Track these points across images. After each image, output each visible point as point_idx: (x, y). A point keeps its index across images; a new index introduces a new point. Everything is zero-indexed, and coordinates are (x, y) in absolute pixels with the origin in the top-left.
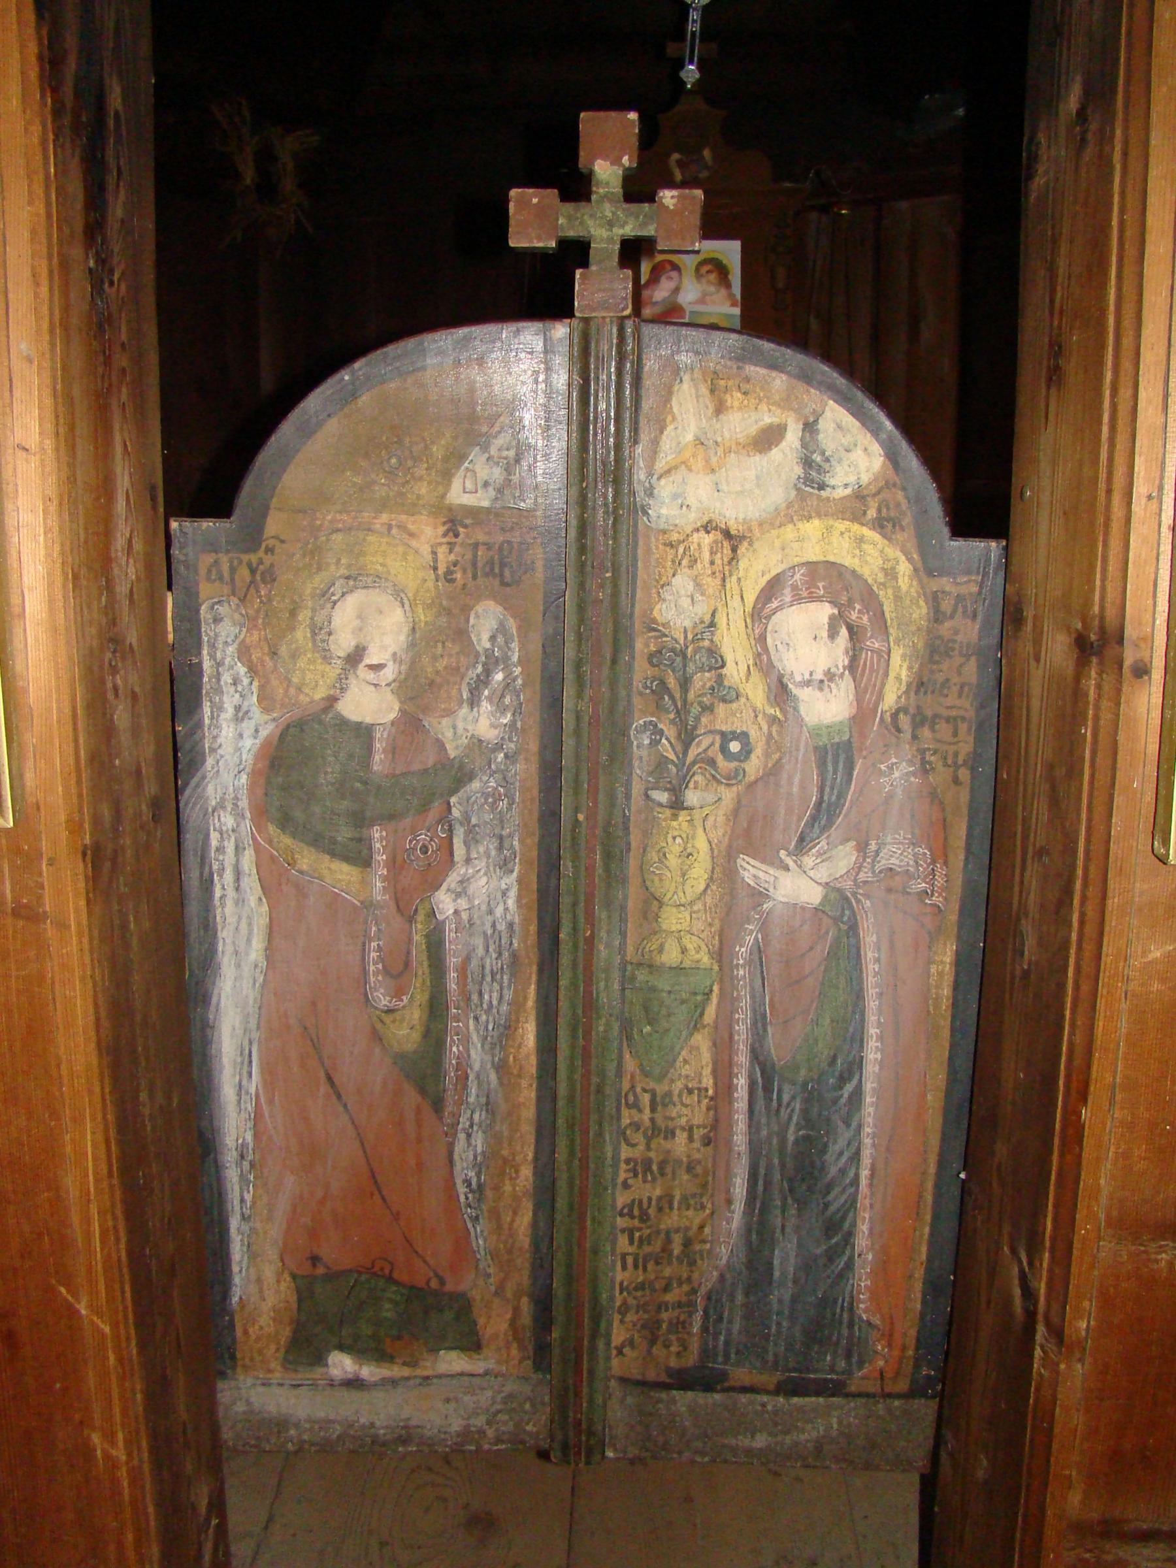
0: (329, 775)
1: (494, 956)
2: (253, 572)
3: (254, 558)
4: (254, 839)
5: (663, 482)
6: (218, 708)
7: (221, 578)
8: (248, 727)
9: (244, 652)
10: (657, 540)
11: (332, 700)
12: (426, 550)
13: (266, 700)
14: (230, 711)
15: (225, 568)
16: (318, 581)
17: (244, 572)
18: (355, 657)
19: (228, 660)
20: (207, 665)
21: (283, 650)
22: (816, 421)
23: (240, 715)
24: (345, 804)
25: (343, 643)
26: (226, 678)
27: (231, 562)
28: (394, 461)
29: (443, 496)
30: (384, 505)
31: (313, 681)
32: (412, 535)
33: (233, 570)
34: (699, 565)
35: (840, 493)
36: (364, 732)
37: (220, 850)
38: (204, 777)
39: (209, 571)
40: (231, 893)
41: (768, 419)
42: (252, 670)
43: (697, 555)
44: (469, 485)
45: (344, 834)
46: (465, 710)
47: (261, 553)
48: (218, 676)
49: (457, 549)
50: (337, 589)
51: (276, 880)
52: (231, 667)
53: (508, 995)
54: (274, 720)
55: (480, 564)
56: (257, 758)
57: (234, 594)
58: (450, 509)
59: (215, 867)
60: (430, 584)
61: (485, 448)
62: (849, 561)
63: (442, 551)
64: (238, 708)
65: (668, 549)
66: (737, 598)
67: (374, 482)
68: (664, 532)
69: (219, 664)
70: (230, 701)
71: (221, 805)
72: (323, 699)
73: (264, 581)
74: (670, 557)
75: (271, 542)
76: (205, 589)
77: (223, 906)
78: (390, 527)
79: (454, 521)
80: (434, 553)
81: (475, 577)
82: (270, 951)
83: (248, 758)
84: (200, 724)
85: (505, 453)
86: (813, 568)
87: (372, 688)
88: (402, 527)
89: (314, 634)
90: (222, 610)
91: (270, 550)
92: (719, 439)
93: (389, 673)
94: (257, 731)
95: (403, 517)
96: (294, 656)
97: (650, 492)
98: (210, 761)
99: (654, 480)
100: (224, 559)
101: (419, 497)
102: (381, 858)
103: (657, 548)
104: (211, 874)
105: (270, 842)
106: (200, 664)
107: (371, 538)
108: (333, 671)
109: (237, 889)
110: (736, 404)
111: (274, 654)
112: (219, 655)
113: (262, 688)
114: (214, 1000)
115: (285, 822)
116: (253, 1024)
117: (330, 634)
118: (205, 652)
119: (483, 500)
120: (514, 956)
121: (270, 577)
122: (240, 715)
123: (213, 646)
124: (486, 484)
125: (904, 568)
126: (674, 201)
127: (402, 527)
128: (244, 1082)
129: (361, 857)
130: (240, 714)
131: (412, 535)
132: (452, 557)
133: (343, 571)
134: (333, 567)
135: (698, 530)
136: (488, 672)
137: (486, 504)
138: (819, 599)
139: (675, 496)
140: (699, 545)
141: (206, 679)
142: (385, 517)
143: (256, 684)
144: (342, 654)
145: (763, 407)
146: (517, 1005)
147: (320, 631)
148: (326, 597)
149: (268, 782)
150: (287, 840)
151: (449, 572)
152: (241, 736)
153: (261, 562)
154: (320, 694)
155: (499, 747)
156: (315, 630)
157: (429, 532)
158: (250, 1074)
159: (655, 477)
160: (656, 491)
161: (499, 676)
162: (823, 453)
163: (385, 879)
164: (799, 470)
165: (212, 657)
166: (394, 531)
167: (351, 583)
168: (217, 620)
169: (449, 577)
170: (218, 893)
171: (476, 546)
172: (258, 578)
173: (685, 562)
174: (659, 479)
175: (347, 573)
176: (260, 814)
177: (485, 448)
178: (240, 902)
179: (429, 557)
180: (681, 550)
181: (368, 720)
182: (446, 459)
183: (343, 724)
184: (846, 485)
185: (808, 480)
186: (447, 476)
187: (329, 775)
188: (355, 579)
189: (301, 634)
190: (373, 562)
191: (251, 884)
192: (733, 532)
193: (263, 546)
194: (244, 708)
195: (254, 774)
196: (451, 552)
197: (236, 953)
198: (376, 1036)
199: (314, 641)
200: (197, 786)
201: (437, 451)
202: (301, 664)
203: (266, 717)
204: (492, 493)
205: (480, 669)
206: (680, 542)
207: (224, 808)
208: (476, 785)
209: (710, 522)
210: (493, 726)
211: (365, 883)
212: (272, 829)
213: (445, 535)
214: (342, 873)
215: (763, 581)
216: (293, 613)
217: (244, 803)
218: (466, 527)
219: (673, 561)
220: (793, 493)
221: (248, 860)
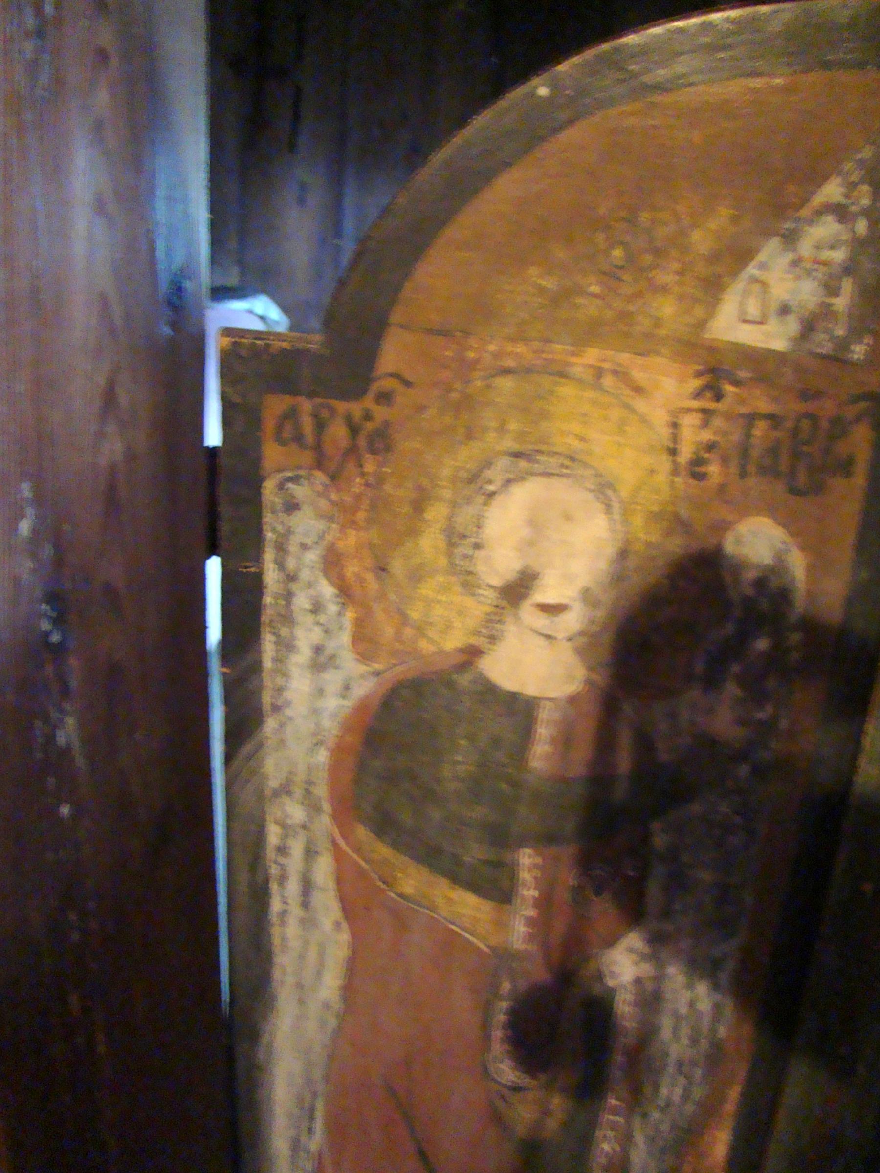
0: (459, 763)
1: (685, 1041)
2: (354, 430)
3: (356, 409)
4: (334, 843)
6: (287, 646)
7: (298, 439)
8: (333, 679)
9: (332, 563)
11: (473, 653)
12: (660, 418)
13: (365, 642)
14: (303, 655)
15: (308, 425)
16: (465, 457)
17: (338, 432)
18: (517, 590)
19: (305, 575)
20: (271, 576)
21: (397, 566)
23: (321, 660)
24: (479, 813)
25: (500, 563)
26: (302, 601)
27: (316, 416)
28: (618, 253)
29: (702, 324)
30: (591, 333)
31: (444, 621)
32: (638, 390)
33: (320, 426)
36: (520, 709)
37: (282, 850)
38: (260, 746)
39: (280, 428)
40: (296, 911)
42: (345, 592)
44: (753, 309)
45: (475, 852)
46: (694, 694)
47: (368, 402)
48: (289, 596)
49: (717, 422)
50: (496, 474)
51: (360, 901)
52: (310, 585)
53: (698, 1093)
54: (377, 674)
55: (755, 453)
56: (347, 727)
57: (319, 465)
58: (712, 349)
59: (274, 870)
60: (662, 478)
61: (790, 239)
63: (689, 422)
64: (318, 649)
67: (580, 291)
69: (292, 578)
70: (306, 637)
71: (285, 789)
72: (461, 651)
73: (373, 452)
75: (388, 384)
77: (283, 923)
78: (599, 373)
79: (717, 371)
80: (675, 425)
81: (743, 474)
82: (348, 989)
83: (330, 727)
84: (256, 667)
85: (827, 255)
87: (542, 642)
88: (620, 374)
89: (451, 545)
90: (300, 491)
91: (385, 398)
93: (573, 621)
94: (347, 688)
95: (624, 357)
96: (417, 576)
98: (270, 724)
100: (306, 406)
101: (658, 322)
102: (529, 892)
104: (267, 881)
105: (358, 850)
106: (258, 578)
107: (566, 390)
108: (478, 608)
109: (305, 905)
111: (382, 569)
112: (291, 564)
113: (359, 623)
114: (265, 1039)
115: (384, 825)
116: (318, 1074)
117: (477, 546)
118: (269, 555)
119: (776, 337)
120: (717, 1046)
121: (381, 442)
122: (321, 660)
123: (281, 548)
124: (784, 310)
127: (620, 374)
128: (304, 1138)
129: (497, 887)
130: (322, 659)
131: (638, 390)
132: (706, 436)
133: (509, 444)
134: (491, 436)
136: (744, 637)
137: (779, 345)
141: (268, 599)
142: (592, 355)
143: (350, 615)
144: (496, 581)
146: (709, 1110)
147: (460, 540)
148: (476, 485)
149: (362, 767)
150: (384, 851)
151: (697, 462)
152: (320, 692)
153: (368, 416)
154: (453, 642)
155: (741, 755)
156: (453, 537)
157: (670, 386)
158: (310, 1131)
161: (762, 644)
163: (530, 922)
165: (281, 565)
166: (608, 381)
167: (523, 464)
168: (292, 507)
169: (696, 470)
170: (276, 905)
171: (751, 419)
172: (362, 442)
175: (516, 447)
176: (346, 809)
178: (308, 923)
179: (665, 432)
181: (531, 690)
182: (714, 258)
183: (489, 692)
186: (713, 288)
187: (459, 763)
188: (526, 457)
189: (429, 543)
190: (564, 431)
191: (328, 906)
194: (329, 651)
195: (339, 750)
196: (705, 424)
197: (299, 986)
198: (497, 1119)
199: (450, 555)
200: (250, 757)
201: (701, 240)
202: (427, 589)
203: (363, 668)
204: (793, 326)
205: (730, 628)
207: (289, 793)
208: (696, 808)
210: (741, 722)
211: (501, 925)
212: (362, 833)
213: (698, 395)
214: (466, 908)
216: (418, 506)
217: (321, 791)
218: (736, 383)
221: (324, 869)
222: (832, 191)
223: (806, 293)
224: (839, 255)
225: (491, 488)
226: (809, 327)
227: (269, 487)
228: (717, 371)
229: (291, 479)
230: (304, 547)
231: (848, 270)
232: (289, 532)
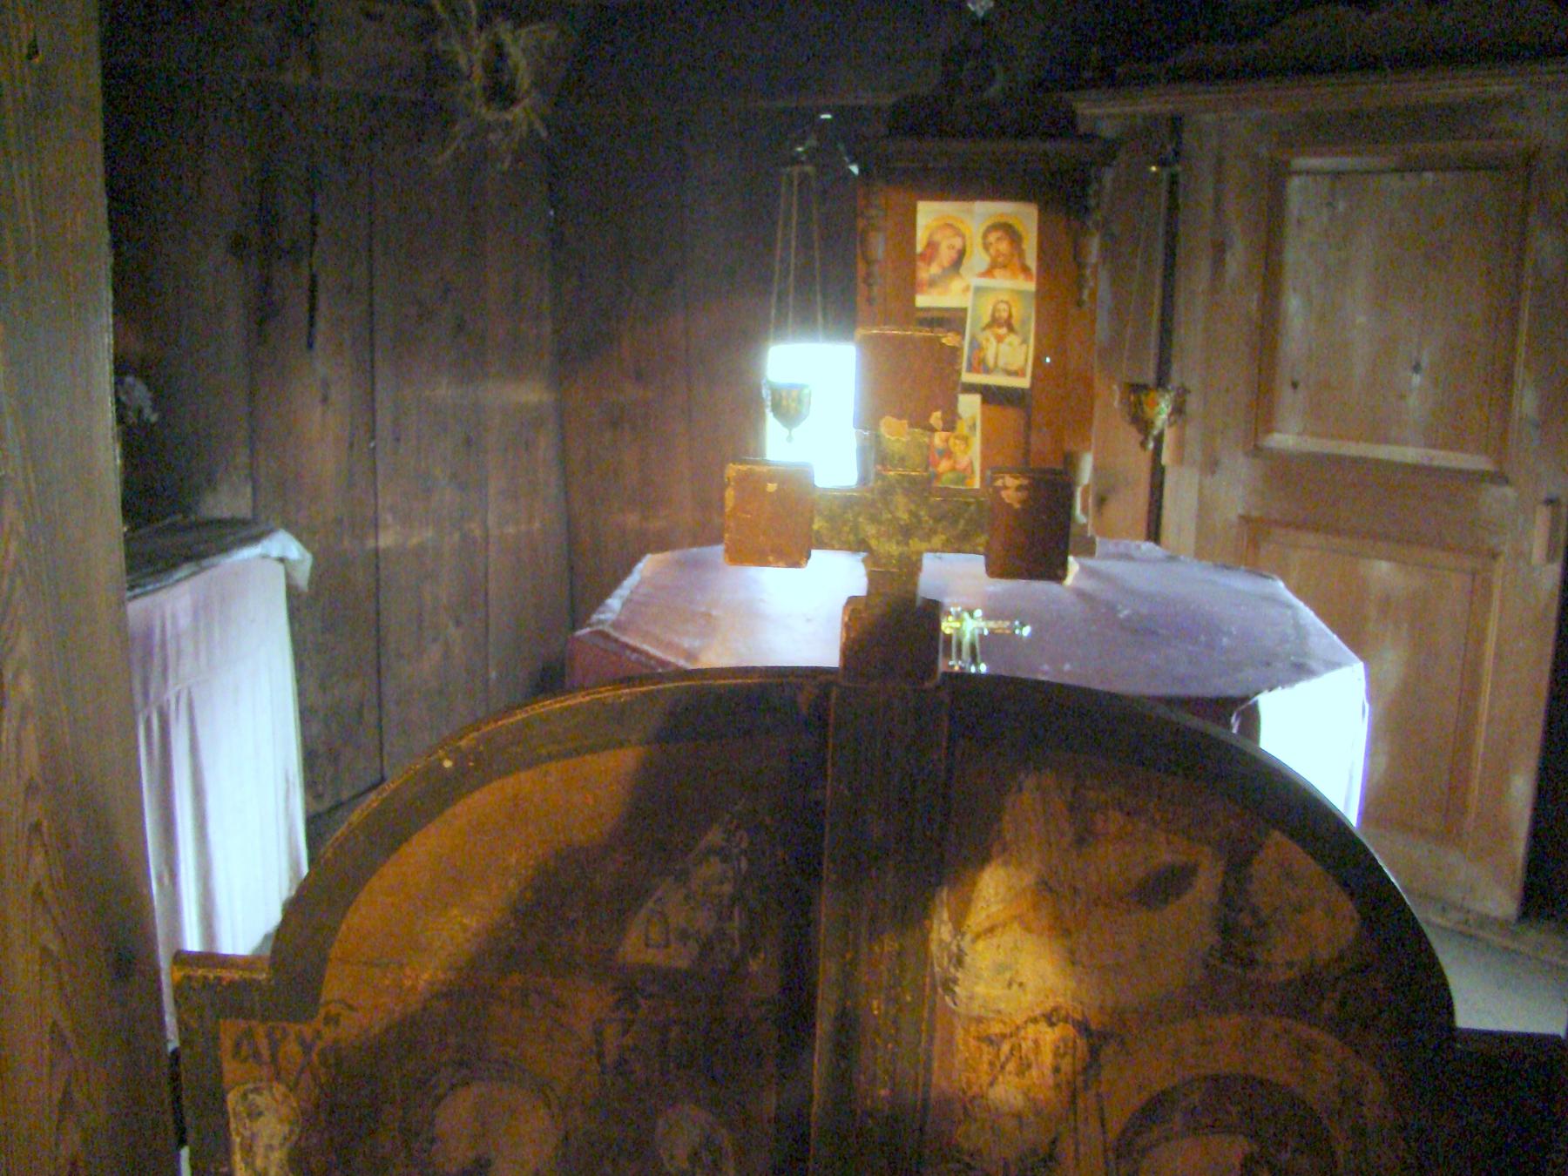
3: (308, 1030)
5: (980, 945)
7: (257, 1055)
10: (967, 1031)
22: (1248, 862)
27: (269, 1035)
33: (274, 1046)
34: (1034, 1072)
35: (1281, 975)
39: (238, 1045)
41: (1165, 854)
43: (1032, 1057)
44: (655, 934)
47: (318, 1022)
57: (278, 1077)
61: (682, 877)
62: (1281, 1076)
63: (611, 1032)
65: (984, 1046)
66: (1094, 1124)
68: (979, 1020)
74: (986, 1058)
76: (230, 1067)
86: (1218, 1084)
90: (261, 1100)
92: (1080, 885)
97: (959, 961)
99: (966, 943)
103: (966, 1043)
110: (1113, 828)
118: (237, 1157)
119: (680, 958)
123: (248, 1149)
124: (684, 935)
125: (1375, 1090)
126: (1022, 495)
132: (628, 1041)
135: (1035, 1021)
137: (683, 964)
138: (1230, 1130)
139: (1000, 968)
140: (1036, 1042)
142: (516, 979)
145: (1161, 837)
151: (621, 1062)
157: (588, 1003)
159: (968, 937)
160: (968, 959)
162: (1255, 912)
164: (1211, 938)
166: (533, 997)
168: (254, 1114)
173: (1011, 1067)
174: (977, 937)
177: (682, 877)
180: (1006, 1048)
184: (1290, 965)
185: (1227, 952)
192: (1093, 1027)
193: (322, 1011)
196: (625, 1032)
204: (694, 948)
206: (1004, 1036)
209: (1056, 1009)
213: (619, 1002)
215: (1137, 1101)
219: (991, 1064)
220: (1198, 973)
222: (715, 836)
223: (704, 922)
224: (727, 888)
225: (440, 1091)
226: (707, 947)
227: (232, 1098)
228: (629, 989)
229: (252, 1091)
230: (270, 1147)
231: (734, 900)
232: (253, 1136)
